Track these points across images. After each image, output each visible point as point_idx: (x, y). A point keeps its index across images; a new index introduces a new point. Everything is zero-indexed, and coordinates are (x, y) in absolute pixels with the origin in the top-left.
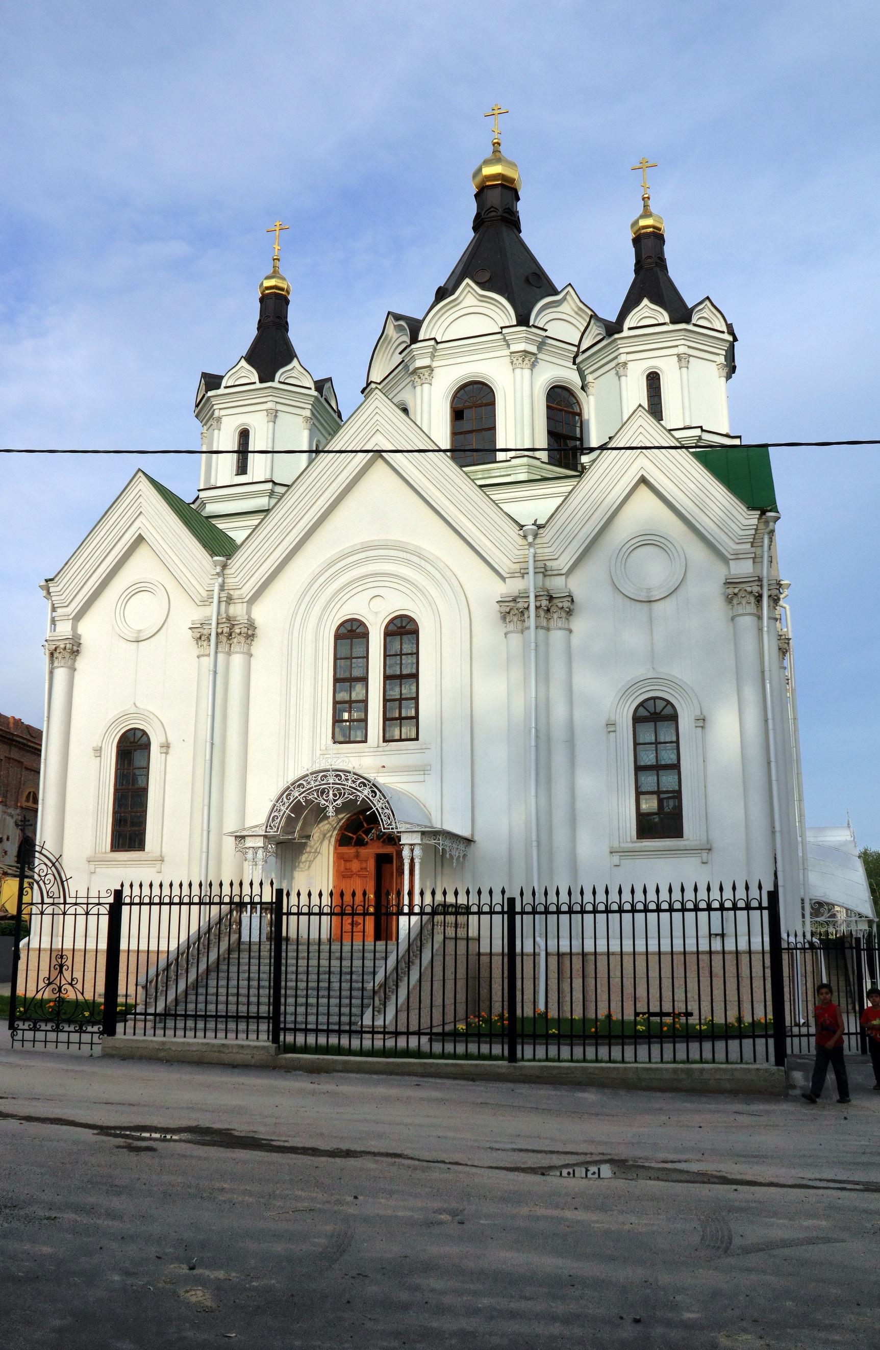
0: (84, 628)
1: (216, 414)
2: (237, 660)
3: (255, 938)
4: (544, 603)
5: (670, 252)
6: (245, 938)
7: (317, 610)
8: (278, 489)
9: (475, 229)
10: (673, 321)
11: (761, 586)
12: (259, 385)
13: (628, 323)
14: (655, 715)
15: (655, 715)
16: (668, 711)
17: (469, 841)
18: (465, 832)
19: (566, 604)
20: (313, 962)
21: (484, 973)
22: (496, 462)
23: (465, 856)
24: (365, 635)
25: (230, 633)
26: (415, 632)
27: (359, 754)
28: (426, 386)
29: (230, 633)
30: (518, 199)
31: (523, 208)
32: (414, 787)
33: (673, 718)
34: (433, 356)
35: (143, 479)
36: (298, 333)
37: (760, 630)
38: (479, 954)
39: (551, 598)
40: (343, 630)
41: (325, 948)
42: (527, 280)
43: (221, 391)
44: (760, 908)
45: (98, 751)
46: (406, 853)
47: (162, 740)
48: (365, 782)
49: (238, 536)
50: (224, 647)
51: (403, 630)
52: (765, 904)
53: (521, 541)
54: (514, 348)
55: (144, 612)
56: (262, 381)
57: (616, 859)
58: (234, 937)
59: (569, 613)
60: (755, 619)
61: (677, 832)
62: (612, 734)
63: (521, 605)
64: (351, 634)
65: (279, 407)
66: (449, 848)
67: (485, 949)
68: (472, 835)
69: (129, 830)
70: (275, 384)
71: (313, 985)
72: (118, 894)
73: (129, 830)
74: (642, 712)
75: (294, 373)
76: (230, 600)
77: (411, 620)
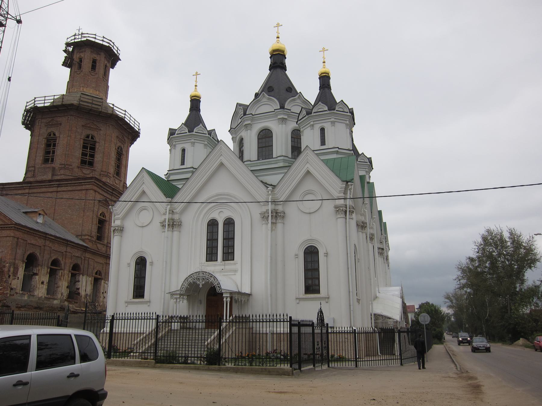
1: (174, 143)
4: (274, 214)
5: (332, 83)
6: (173, 328)
7: (202, 216)
8: (194, 170)
9: (270, 70)
10: (329, 110)
11: (346, 208)
12: (188, 134)
13: (313, 111)
16: (316, 250)
17: (249, 295)
18: (248, 291)
19: (282, 214)
20: (194, 336)
21: (254, 340)
22: (273, 158)
23: (248, 300)
24: (218, 224)
26: (234, 223)
27: (215, 265)
29: (173, 224)
30: (286, 58)
31: (287, 62)
32: (230, 278)
33: (317, 252)
35: (144, 171)
36: (204, 113)
37: (346, 222)
38: (253, 333)
39: (276, 213)
40: (210, 223)
41: (179, 332)
42: (287, 90)
43: (176, 135)
44: (287, 321)
45: (129, 264)
46: (225, 299)
47: (151, 261)
48: (212, 276)
49: (180, 187)
50: (171, 229)
51: (229, 223)
52: (288, 320)
53: (267, 193)
54: (279, 117)
55: (145, 217)
57: (298, 301)
58: (170, 328)
59: (283, 217)
60: (344, 219)
61: (318, 292)
62: (297, 259)
63: (266, 215)
64: (212, 224)
65: (196, 141)
66: (240, 298)
67: (254, 332)
69: (139, 291)
70: (194, 133)
71: (190, 344)
72: (113, 316)
73: (139, 291)
77: (232, 219)
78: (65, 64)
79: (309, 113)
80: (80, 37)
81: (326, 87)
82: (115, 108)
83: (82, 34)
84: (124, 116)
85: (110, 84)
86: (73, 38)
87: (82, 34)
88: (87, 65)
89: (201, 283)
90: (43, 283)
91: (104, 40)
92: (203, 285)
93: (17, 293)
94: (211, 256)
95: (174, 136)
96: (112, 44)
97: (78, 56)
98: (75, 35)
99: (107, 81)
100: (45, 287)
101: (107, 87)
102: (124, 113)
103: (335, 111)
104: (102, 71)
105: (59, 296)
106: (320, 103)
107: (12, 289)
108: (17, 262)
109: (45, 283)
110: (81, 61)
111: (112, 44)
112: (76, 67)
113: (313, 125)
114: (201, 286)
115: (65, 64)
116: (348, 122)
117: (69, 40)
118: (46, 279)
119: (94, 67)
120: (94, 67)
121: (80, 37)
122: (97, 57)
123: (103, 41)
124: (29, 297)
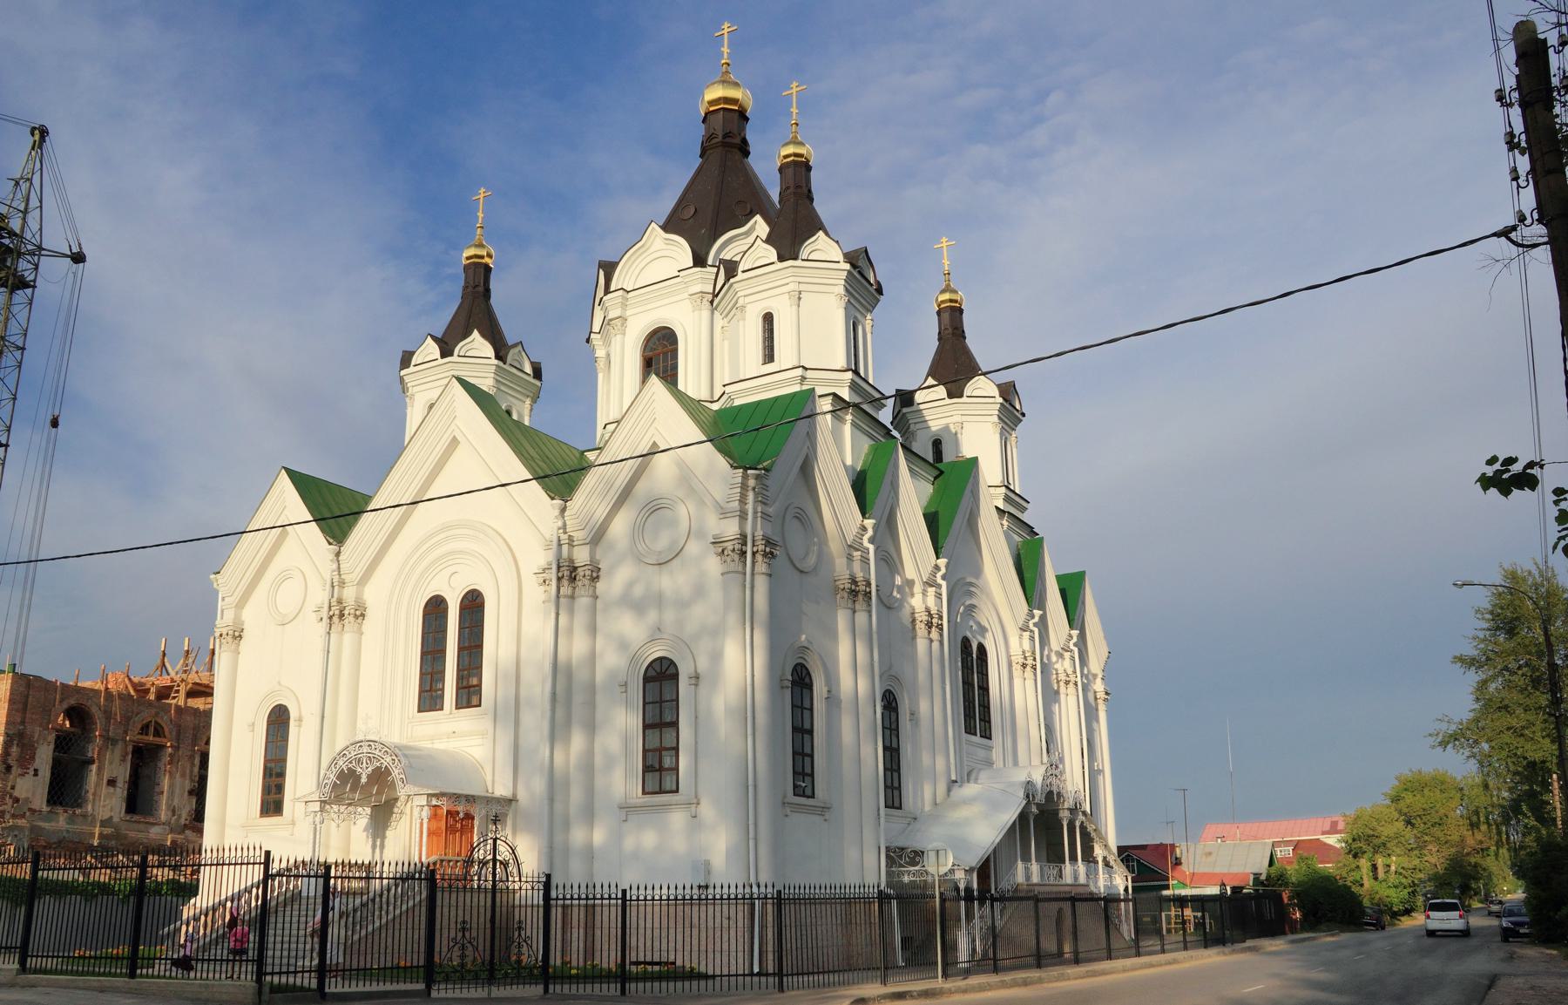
0: (248, 615)
2: (348, 638)
3: (312, 894)
12: (441, 361)
14: (661, 679)
15: (661, 679)
25: (343, 613)
28: (619, 337)
34: (624, 306)
51: (473, 604)
56: (443, 355)
64: (435, 608)
68: (515, 795)
70: (454, 358)
74: (651, 673)
75: (475, 345)
76: (342, 583)
89: (364, 774)
90: (112, 782)
92: (369, 777)
93: (33, 811)
94: (430, 699)
95: (412, 369)
100: (121, 792)
103: (798, 263)
105: (163, 814)
107: (17, 800)
108: (29, 728)
109: (120, 784)
114: (364, 780)
118: (123, 772)
124: (71, 820)
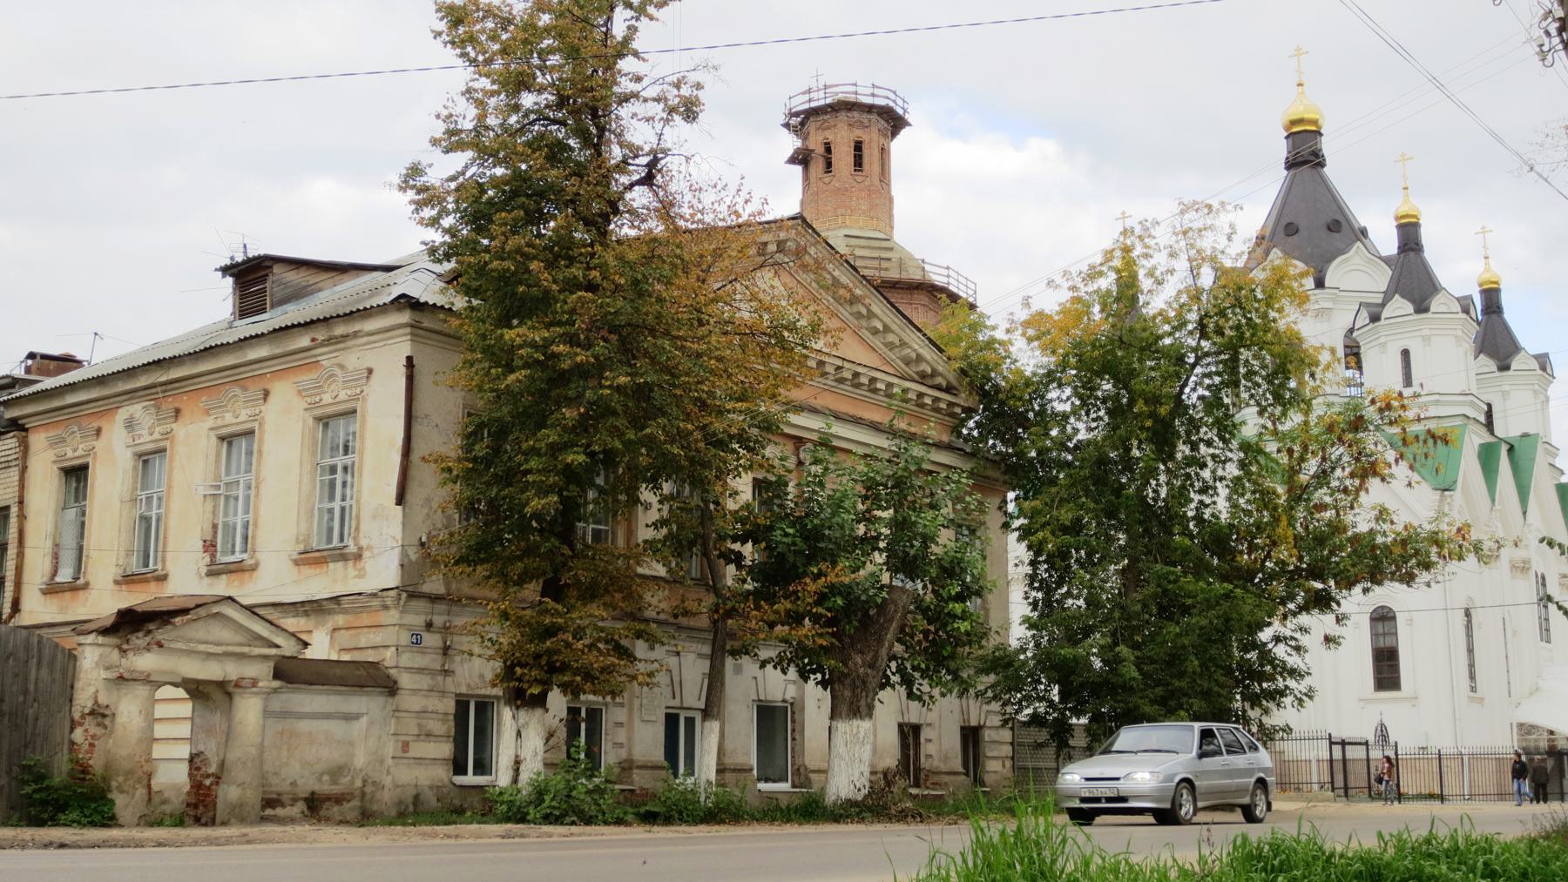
31: (1328, 146)
78: (793, 160)
79: (1375, 318)
80: (821, 94)
81: (1412, 250)
82: (927, 267)
83: (826, 87)
84: (945, 280)
85: (893, 193)
86: (806, 97)
87: (826, 87)
88: (843, 157)
91: (877, 91)
96: (892, 96)
97: (820, 139)
98: (809, 91)
99: (889, 185)
101: (891, 200)
102: (945, 272)
104: (876, 168)
106: (1397, 296)
110: (828, 150)
111: (892, 96)
112: (817, 166)
113: (1384, 345)
115: (793, 160)
116: (1459, 333)
117: (795, 102)
119: (858, 162)
120: (858, 162)
121: (821, 94)
122: (864, 136)
123: (873, 95)
